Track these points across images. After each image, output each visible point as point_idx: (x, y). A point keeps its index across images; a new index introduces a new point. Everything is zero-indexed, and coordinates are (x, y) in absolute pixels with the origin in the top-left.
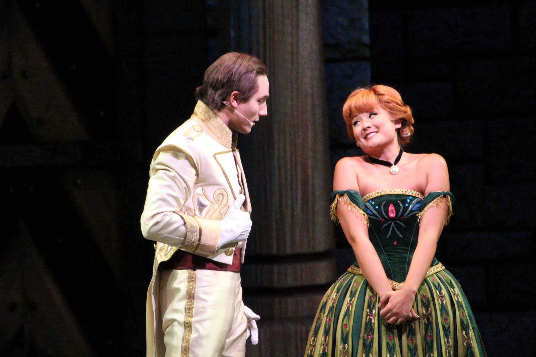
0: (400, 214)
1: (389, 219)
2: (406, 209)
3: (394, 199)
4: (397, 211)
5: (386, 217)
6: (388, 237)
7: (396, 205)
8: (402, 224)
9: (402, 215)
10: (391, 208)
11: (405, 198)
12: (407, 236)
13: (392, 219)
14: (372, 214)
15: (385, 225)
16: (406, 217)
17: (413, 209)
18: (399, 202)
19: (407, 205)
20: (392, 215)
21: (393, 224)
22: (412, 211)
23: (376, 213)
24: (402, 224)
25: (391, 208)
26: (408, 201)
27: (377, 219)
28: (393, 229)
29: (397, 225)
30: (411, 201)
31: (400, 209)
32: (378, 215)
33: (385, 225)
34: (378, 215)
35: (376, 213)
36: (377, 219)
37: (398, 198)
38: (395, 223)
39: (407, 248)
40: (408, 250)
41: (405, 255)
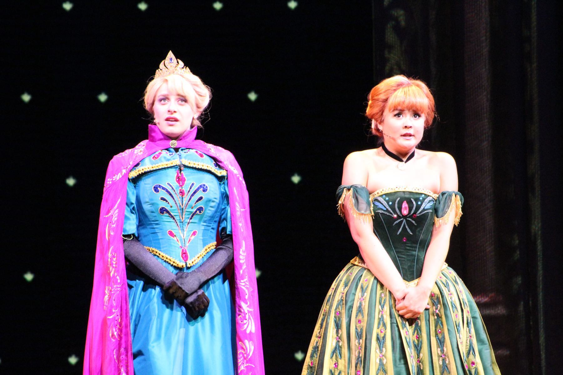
0: (412, 212)
1: (401, 216)
2: (418, 207)
3: (407, 196)
4: (410, 209)
5: (399, 213)
6: (398, 233)
7: (409, 202)
8: (414, 222)
9: (415, 213)
10: (405, 205)
11: (418, 196)
12: (417, 233)
13: (405, 217)
14: (385, 209)
15: (397, 222)
16: (418, 215)
17: (425, 208)
18: (412, 199)
19: (419, 203)
20: (405, 212)
21: (404, 221)
22: (424, 210)
23: (390, 209)
24: (414, 222)
25: (405, 205)
26: (421, 199)
27: (391, 215)
28: (404, 225)
29: (408, 222)
30: (424, 199)
31: (413, 207)
32: (391, 211)
33: (397, 222)
34: (391, 211)
35: (390, 209)
36: (391, 215)
37: (412, 196)
38: (407, 220)
39: (416, 245)
40: (416, 247)
41: (414, 253)
